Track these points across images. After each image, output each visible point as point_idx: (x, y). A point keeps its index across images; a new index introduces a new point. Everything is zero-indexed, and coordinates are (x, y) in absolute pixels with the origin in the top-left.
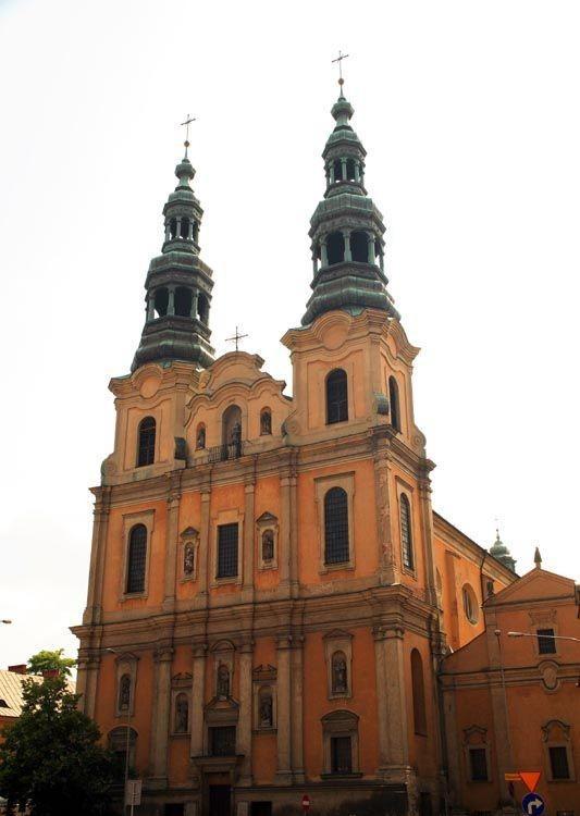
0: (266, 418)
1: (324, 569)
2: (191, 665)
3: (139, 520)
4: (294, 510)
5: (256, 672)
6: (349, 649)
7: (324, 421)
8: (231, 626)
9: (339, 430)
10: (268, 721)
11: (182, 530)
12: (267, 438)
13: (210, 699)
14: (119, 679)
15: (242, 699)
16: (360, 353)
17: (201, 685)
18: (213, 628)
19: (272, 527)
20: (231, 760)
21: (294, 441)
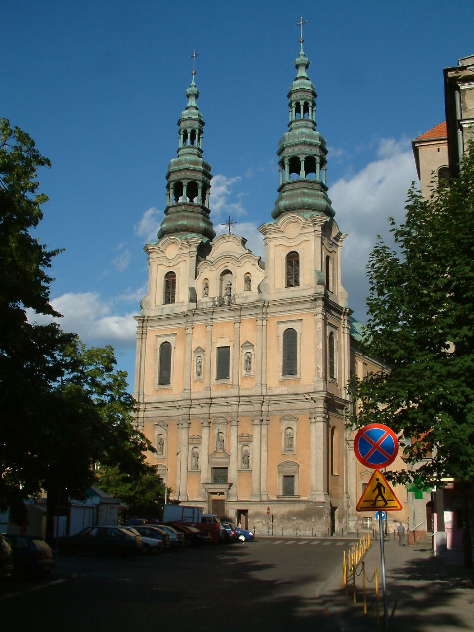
0: (248, 281)
1: (282, 378)
2: (201, 431)
3: (166, 339)
4: (264, 341)
5: (240, 437)
6: (296, 426)
7: (284, 284)
8: (226, 409)
9: (294, 292)
10: (247, 465)
11: (194, 349)
12: (248, 293)
13: (212, 451)
14: (156, 436)
15: (231, 452)
16: (308, 242)
17: (207, 443)
18: (213, 410)
19: (251, 350)
20: (226, 486)
21: (266, 297)
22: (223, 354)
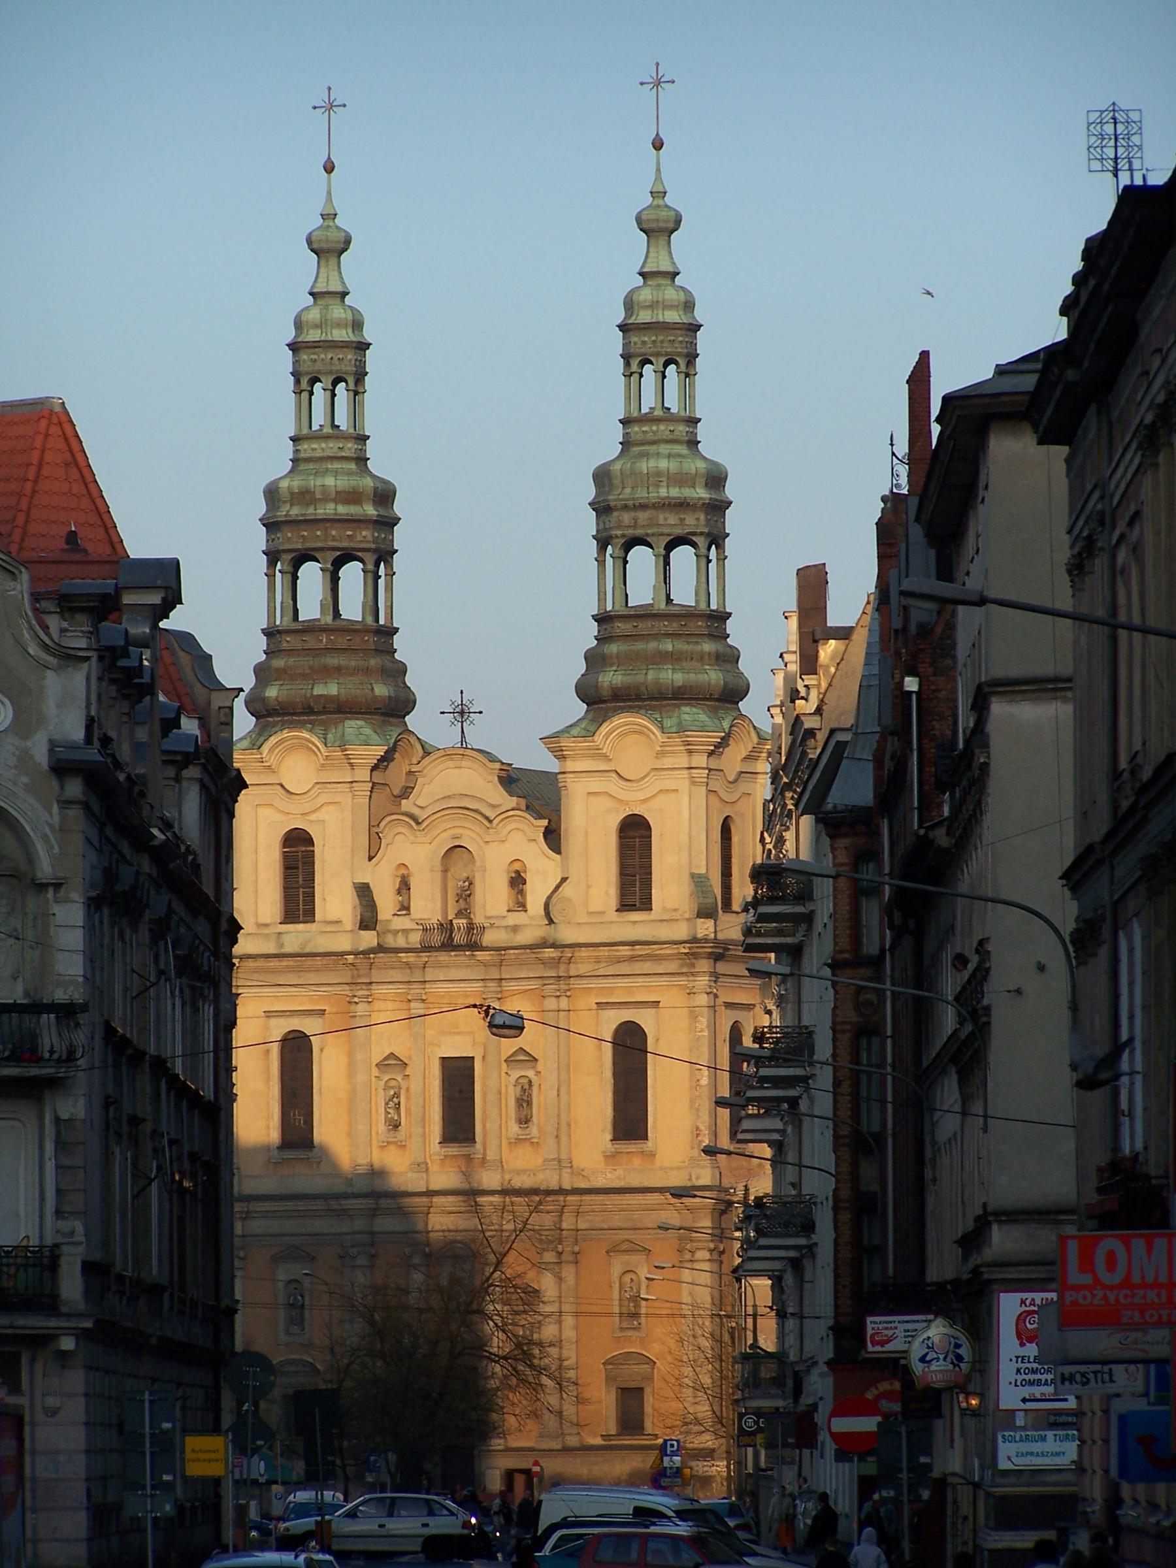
0: (517, 881)
3: (296, 1024)
7: (613, 900)
9: (636, 926)
11: (377, 1058)
12: (517, 918)
16: (673, 795)
19: (530, 1074)
22: (458, 1078)
